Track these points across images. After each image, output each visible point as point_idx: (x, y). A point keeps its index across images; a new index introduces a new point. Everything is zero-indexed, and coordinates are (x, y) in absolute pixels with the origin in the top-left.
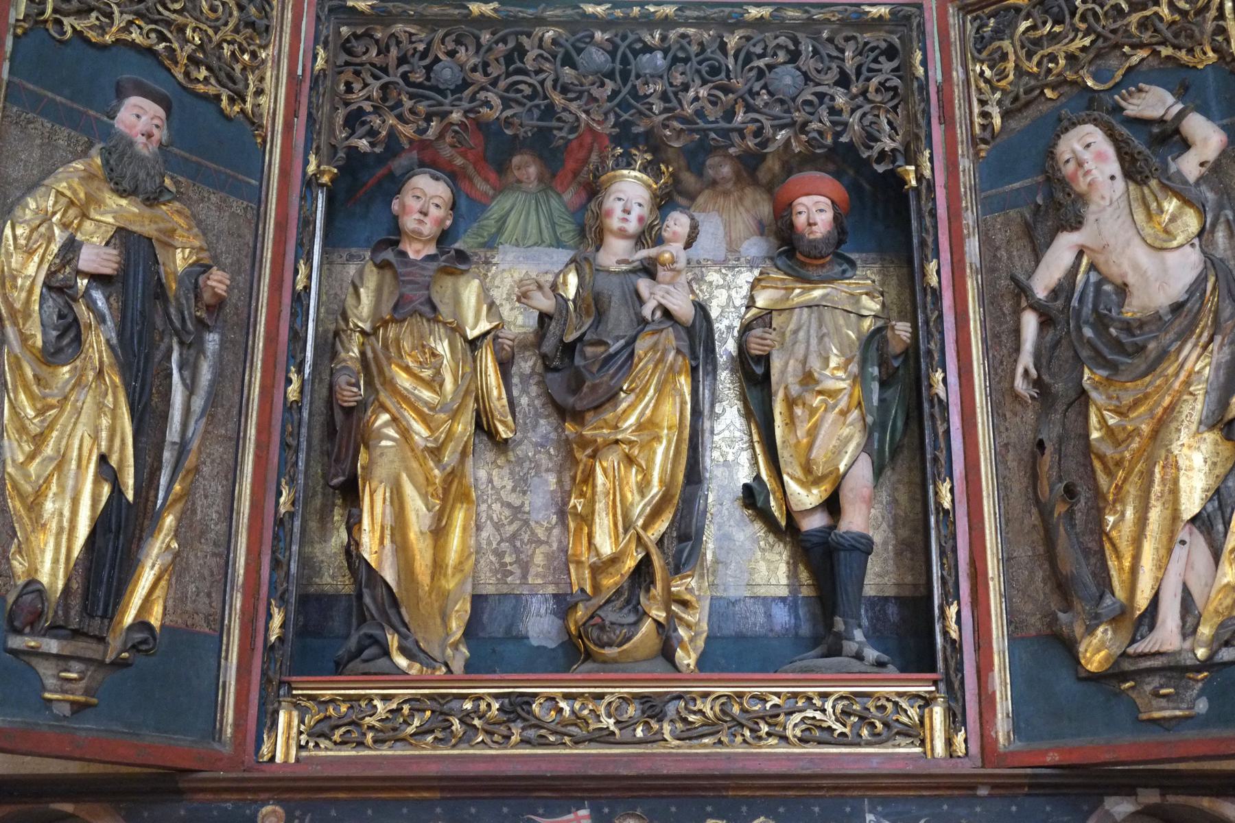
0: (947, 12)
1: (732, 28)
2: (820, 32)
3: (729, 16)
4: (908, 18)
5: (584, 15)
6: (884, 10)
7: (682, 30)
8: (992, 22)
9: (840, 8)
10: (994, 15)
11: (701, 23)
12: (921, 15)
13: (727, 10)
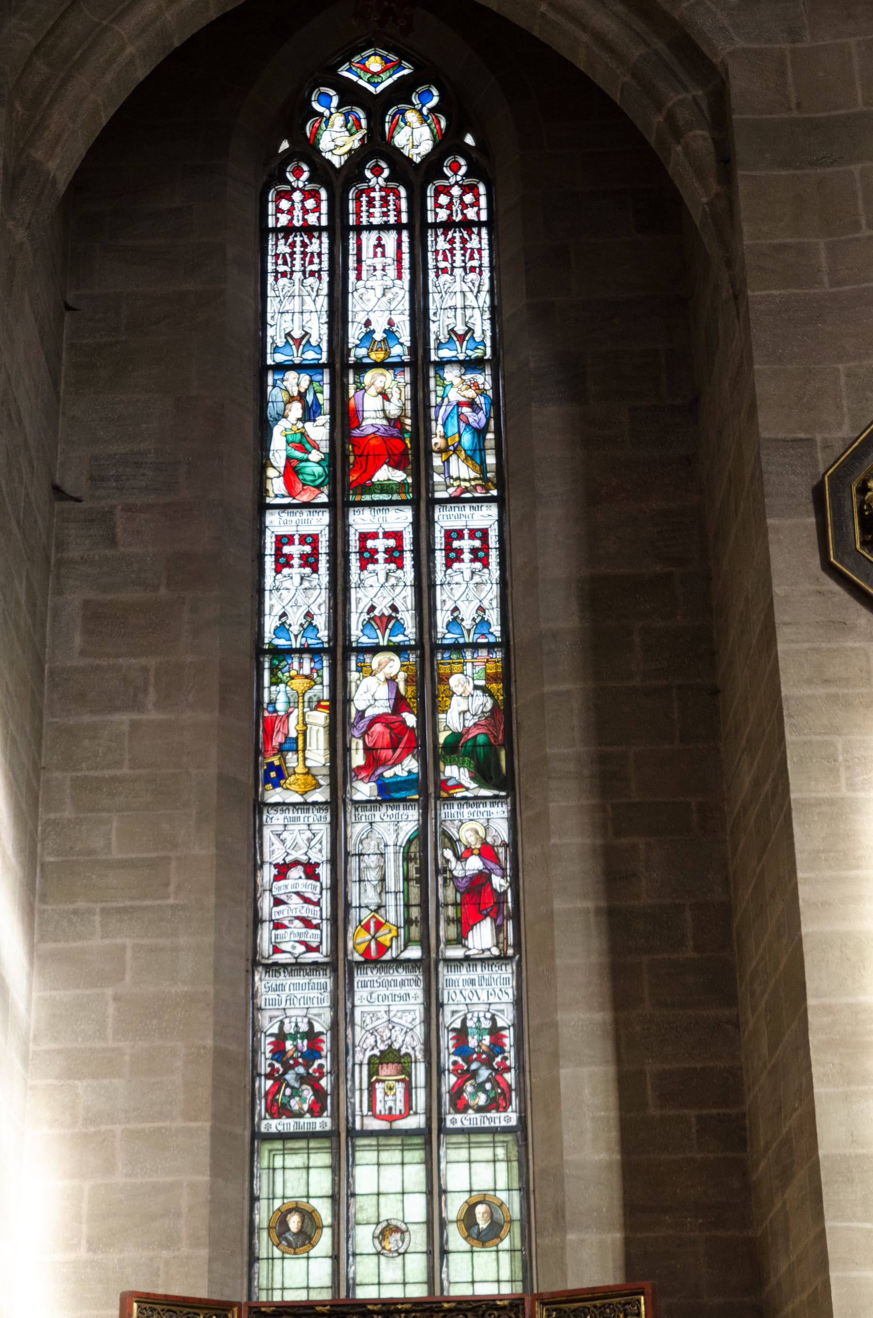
0: (535, 1304)
1: (437, 1312)
2: (477, 1312)
3: (437, 1307)
4: (517, 1305)
5: (369, 1310)
6: (506, 1302)
7: (414, 1314)
8: (554, 1313)
9: (485, 1302)
10: (555, 1310)
11: (421, 1311)
12: (523, 1304)
13: (434, 1305)
